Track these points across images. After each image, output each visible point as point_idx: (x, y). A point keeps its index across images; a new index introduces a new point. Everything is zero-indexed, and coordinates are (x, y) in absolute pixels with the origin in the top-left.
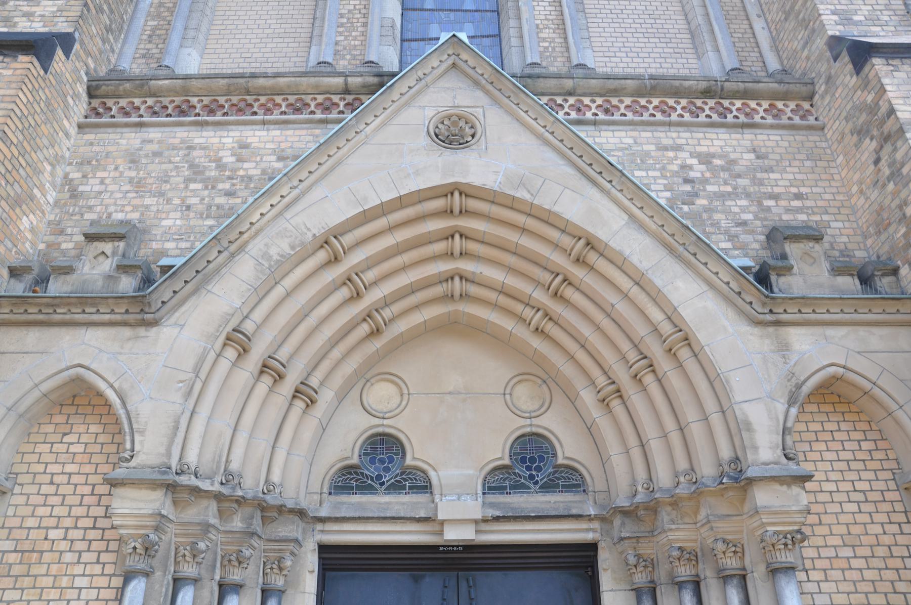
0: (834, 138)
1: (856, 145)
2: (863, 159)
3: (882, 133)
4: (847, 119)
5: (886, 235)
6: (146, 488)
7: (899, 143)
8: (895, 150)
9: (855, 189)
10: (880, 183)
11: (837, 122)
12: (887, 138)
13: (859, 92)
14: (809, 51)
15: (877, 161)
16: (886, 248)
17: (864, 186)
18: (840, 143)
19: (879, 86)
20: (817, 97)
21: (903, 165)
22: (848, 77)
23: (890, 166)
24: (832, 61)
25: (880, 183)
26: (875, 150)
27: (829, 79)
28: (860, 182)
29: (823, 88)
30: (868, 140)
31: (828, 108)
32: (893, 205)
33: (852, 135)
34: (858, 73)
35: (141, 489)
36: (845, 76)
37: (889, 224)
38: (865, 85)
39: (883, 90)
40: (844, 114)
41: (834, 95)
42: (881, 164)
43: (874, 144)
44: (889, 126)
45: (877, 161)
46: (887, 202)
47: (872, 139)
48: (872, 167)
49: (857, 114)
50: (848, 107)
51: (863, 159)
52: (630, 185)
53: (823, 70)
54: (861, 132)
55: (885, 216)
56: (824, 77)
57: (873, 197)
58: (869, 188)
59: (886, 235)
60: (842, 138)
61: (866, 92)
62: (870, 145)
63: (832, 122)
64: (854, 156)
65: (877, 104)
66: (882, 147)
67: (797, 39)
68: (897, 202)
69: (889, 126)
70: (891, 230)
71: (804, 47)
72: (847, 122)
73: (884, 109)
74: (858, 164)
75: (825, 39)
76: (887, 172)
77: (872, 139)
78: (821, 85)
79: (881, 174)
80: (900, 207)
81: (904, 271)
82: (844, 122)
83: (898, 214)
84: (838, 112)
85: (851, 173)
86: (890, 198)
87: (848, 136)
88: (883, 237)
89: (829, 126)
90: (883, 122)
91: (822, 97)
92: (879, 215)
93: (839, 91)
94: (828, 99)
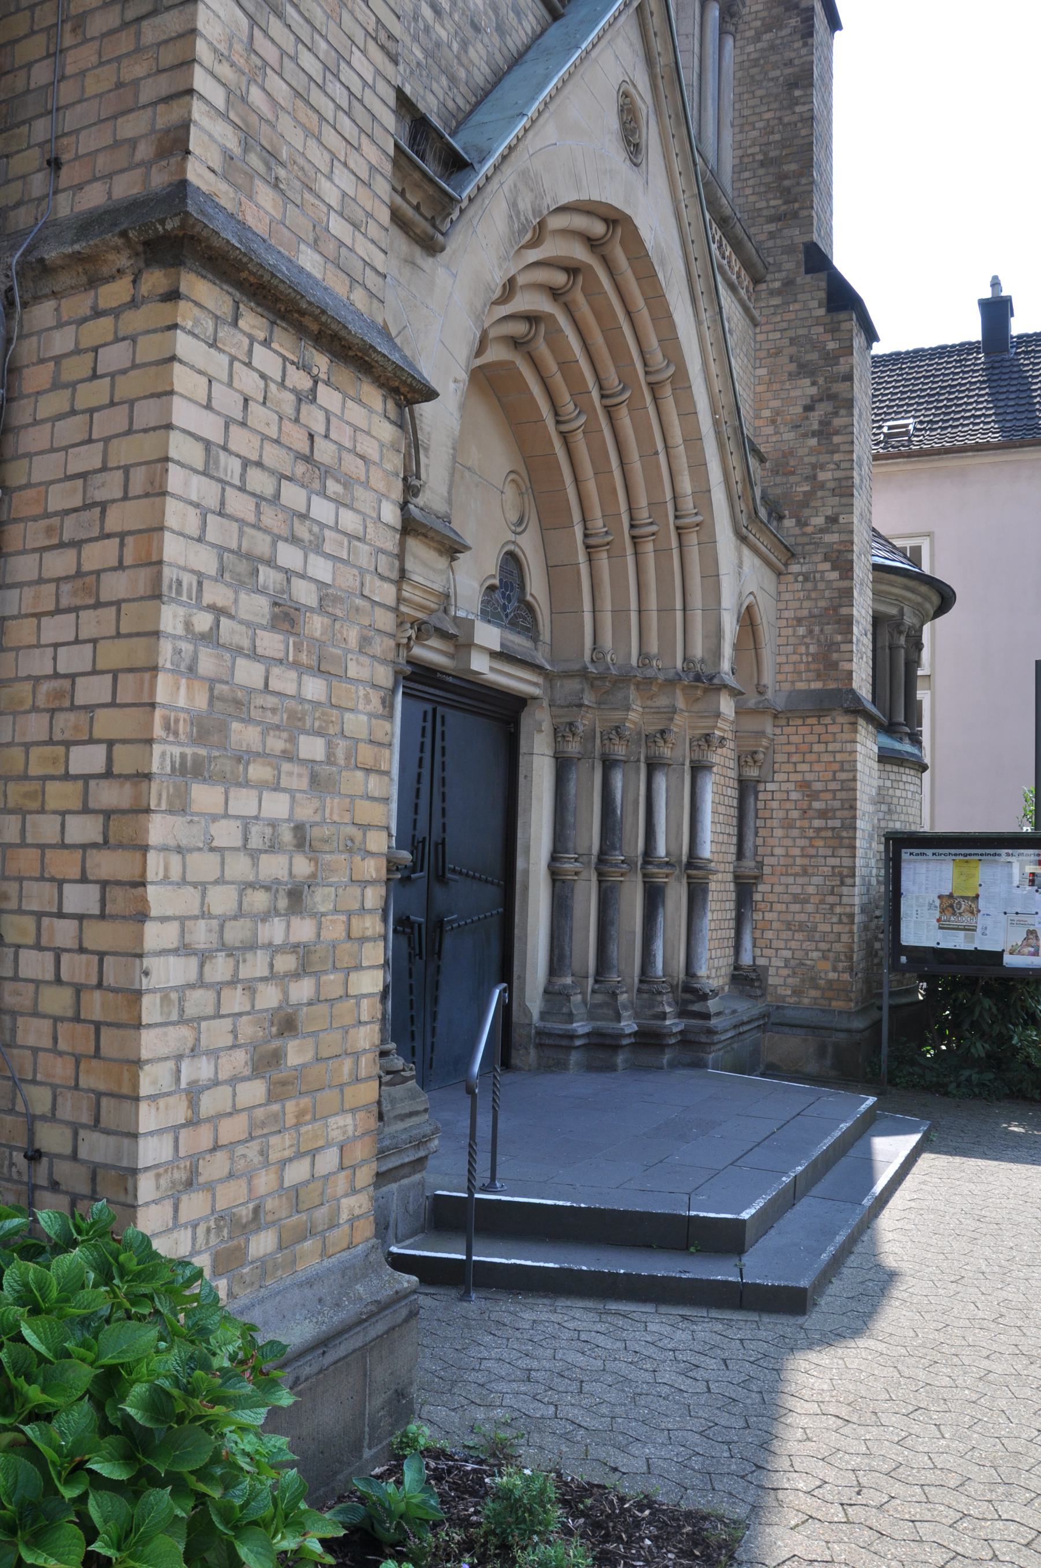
0: (765, 346)
1: (790, 374)
2: (793, 393)
3: (829, 389)
4: (792, 341)
5: (784, 480)
6: (435, 549)
7: (843, 412)
8: (836, 414)
9: (766, 413)
10: (802, 430)
11: (778, 335)
12: (832, 397)
13: (821, 329)
14: (780, 230)
15: (809, 408)
16: (778, 491)
17: (779, 419)
18: (770, 356)
19: (848, 344)
20: (763, 286)
21: (837, 433)
22: (815, 304)
23: (821, 423)
24: (803, 269)
25: (802, 430)
26: (812, 396)
27: (789, 283)
28: (777, 412)
29: (777, 285)
30: (807, 381)
31: (772, 310)
32: (806, 460)
33: (791, 361)
34: (830, 310)
35: (429, 547)
36: (813, 299)
37: (793, 473)
38: (833, 329)
39: (849, 351)
40: (791, 333)
41: (788, 303)
42: (812, 414)
43: (814, 390)
44: (839, 387)
45: (809, 408)
46: (801, 452)
47: (814, 384)
48: (800, 410)
49: (808, 347)
50: (801, 332)
51: (793, 393)
52: (720, 328)
53: (787, 266)
54: (804, 370)
55: (792, 463)
56: (784, 274)
57: (785, 436)
58: (785, 425)
59: (784, 480)
60: (777, 354)
61: (829, 336)
62: (806, 389)
63: (770, 327)
64: (783, 382)
65: (836, 358)
66: (821, 400)
67: (767, 201)
68: (813, 459)
69: (839, 387)
70: (792, 479)
71: (771, 220)
72: (791, 344)
73: (842, 368)
74: (784, 395)
75: (806, 239)
76: (816, 426)
77: (814, 384)
78: (775, 280)
79: (806, 423)
80: (814, 467)
81: (789, 523)
82: (787, 341)
83: (808, 471)
84: (784, 325)
85: (769, 395)
86: (806, 450)
87: (784, 359)
88: (779, 479)
89: (764, 328)
90: (833, 379)
91: (772, 293)
92: (784, 456)
93: (797, 306)
94: (776, 301)
